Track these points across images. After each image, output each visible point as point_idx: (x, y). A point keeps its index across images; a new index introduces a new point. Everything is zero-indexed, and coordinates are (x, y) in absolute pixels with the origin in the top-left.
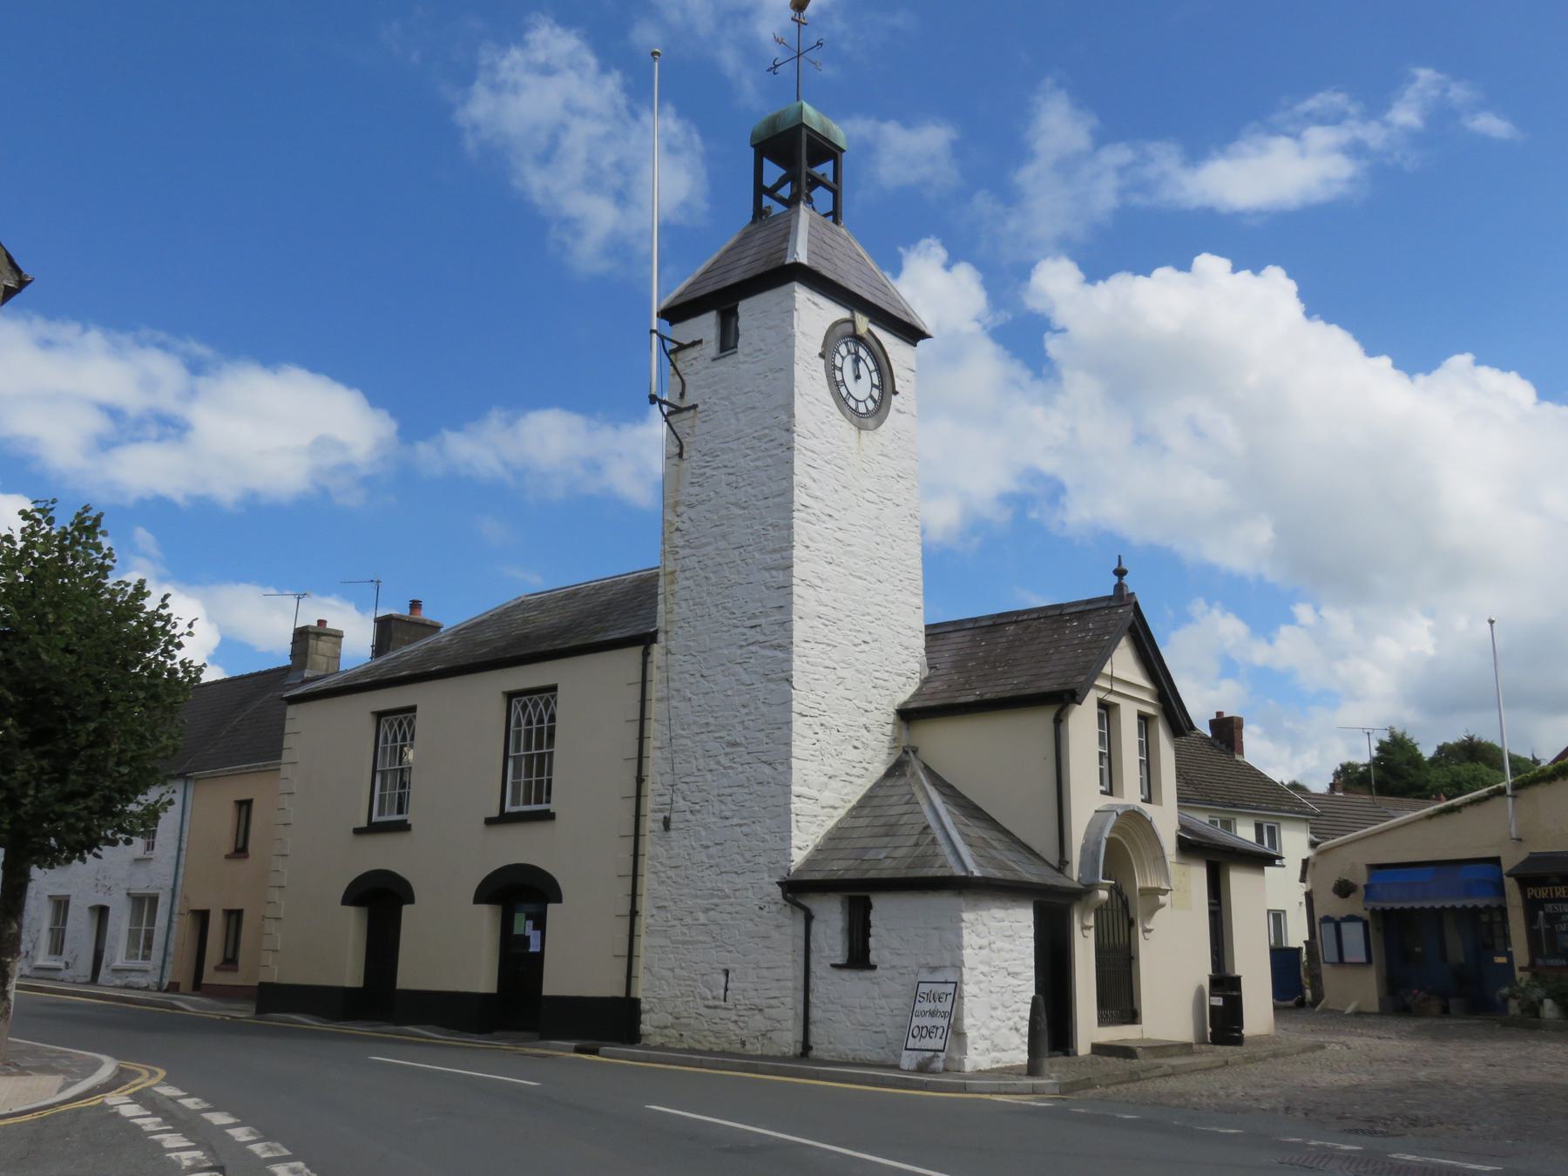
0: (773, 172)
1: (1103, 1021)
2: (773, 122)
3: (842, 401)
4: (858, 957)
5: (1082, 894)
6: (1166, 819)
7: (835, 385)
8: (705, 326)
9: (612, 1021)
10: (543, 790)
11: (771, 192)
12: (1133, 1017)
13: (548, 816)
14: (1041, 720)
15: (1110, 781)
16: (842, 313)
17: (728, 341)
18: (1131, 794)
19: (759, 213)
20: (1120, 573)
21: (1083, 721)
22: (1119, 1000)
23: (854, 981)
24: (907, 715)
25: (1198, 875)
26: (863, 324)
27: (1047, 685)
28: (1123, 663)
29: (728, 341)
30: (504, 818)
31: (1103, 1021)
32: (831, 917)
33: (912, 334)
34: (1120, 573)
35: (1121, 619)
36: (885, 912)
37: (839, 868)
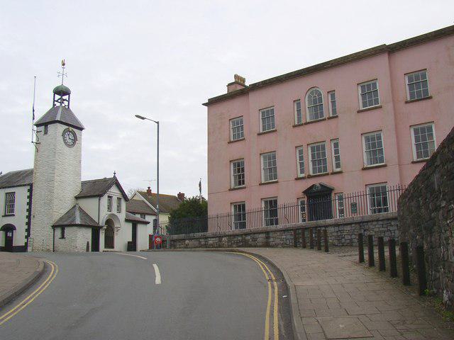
0: (57, 97)
1: (105, 248)
2: (57, 88)
3: (66, 143)
4: (63, 237)
5: (101, 227)
6: (122, 216)
7: (64, 140)
8: (42, 128)
9: (24, 249)
10: (12, 211)
11: (57, 101)
12: (113, 247)
13: (14, 215)
14: (97, 199)
15: (110, 208)
16: (67, 127)
17: (46, 133)
18: (114, 211)
19: (54, 105)
20: (115, 174)
21: (105, 200)
22: (110, 243)
23: (63, 241)
24: (77, 198)
25: (130, 225)
26: (71, 129)
27: (97, 193)
28: (114, 190)
29: (46, 133)
30: (5, 216)
31: (105, 248)
32: (58, 232)
33: (81, 129)
34: (115, 174)
35: (115, 182)
36: (67, 230)
37: (61, 223)
